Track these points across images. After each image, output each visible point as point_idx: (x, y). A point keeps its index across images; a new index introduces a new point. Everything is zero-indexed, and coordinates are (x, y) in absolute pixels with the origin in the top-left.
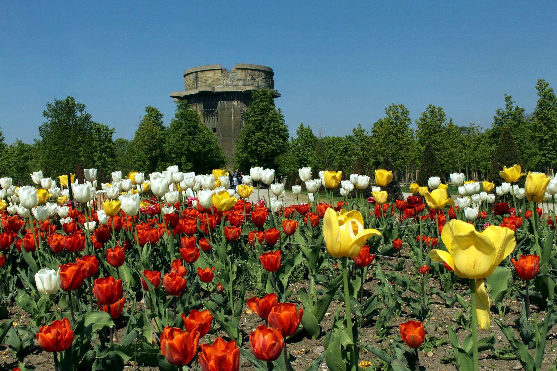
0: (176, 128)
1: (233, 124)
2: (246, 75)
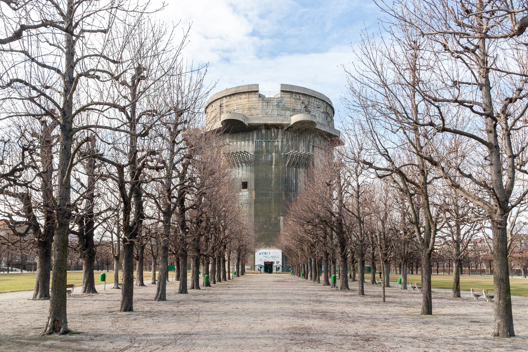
1: (273, 176)
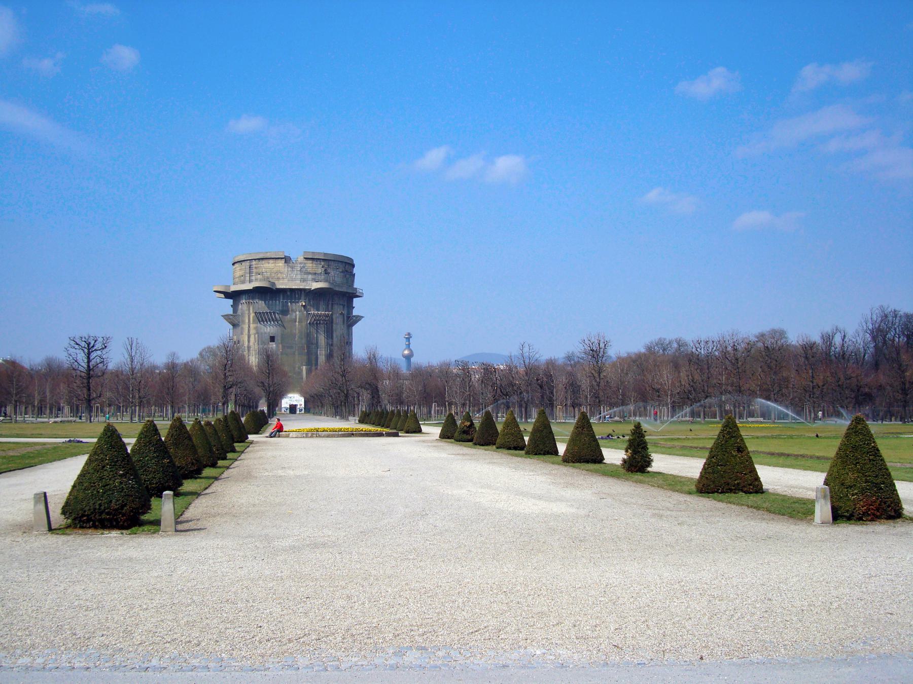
0: (260, 370)
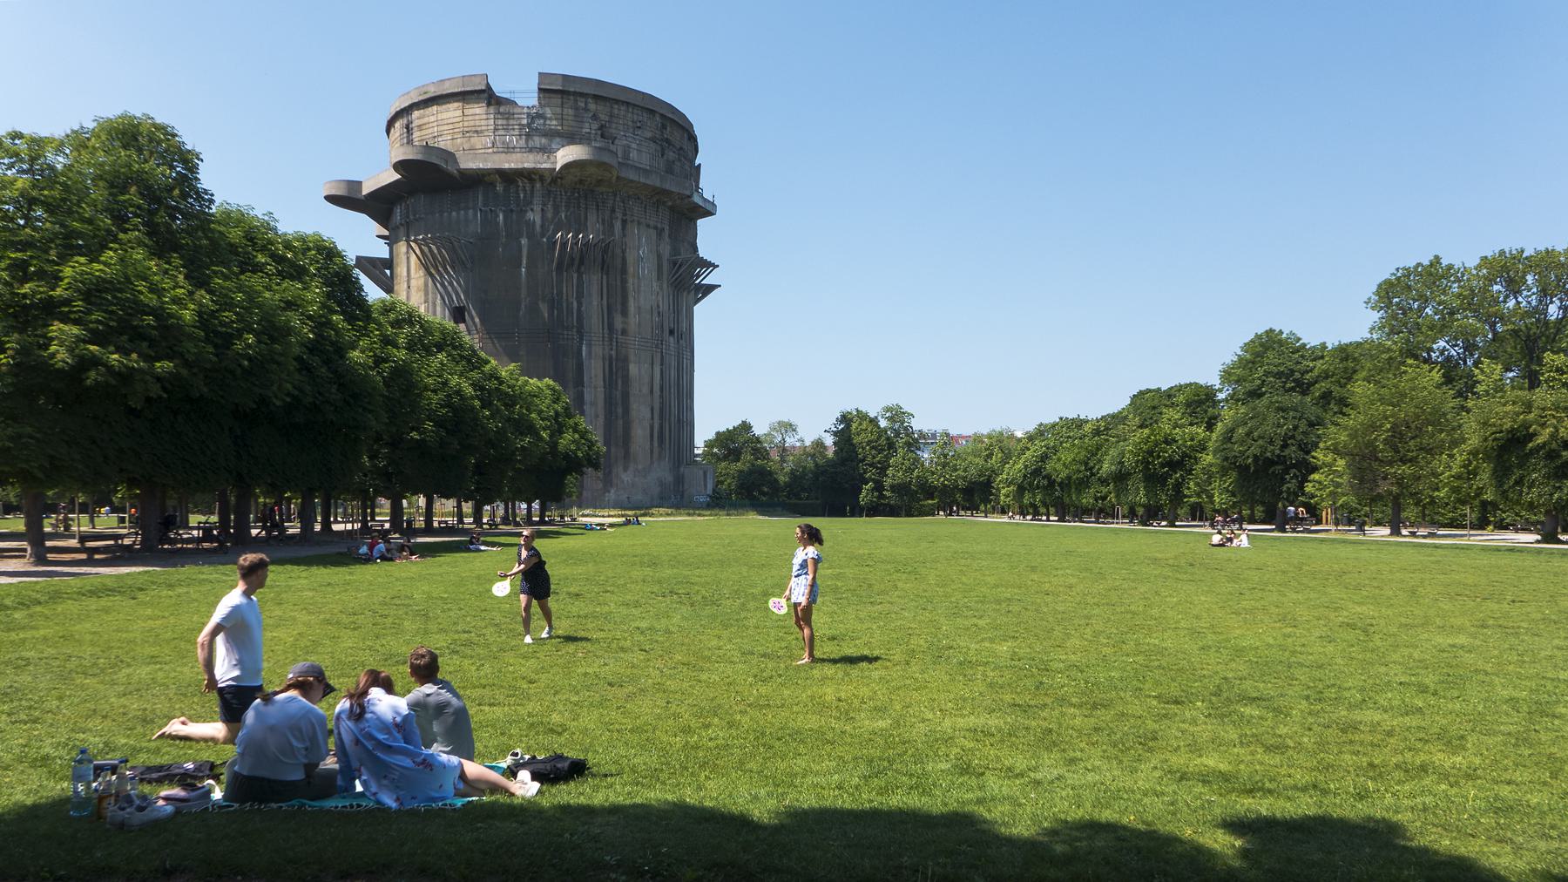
1: (524, 292)
2: (578, 118)
